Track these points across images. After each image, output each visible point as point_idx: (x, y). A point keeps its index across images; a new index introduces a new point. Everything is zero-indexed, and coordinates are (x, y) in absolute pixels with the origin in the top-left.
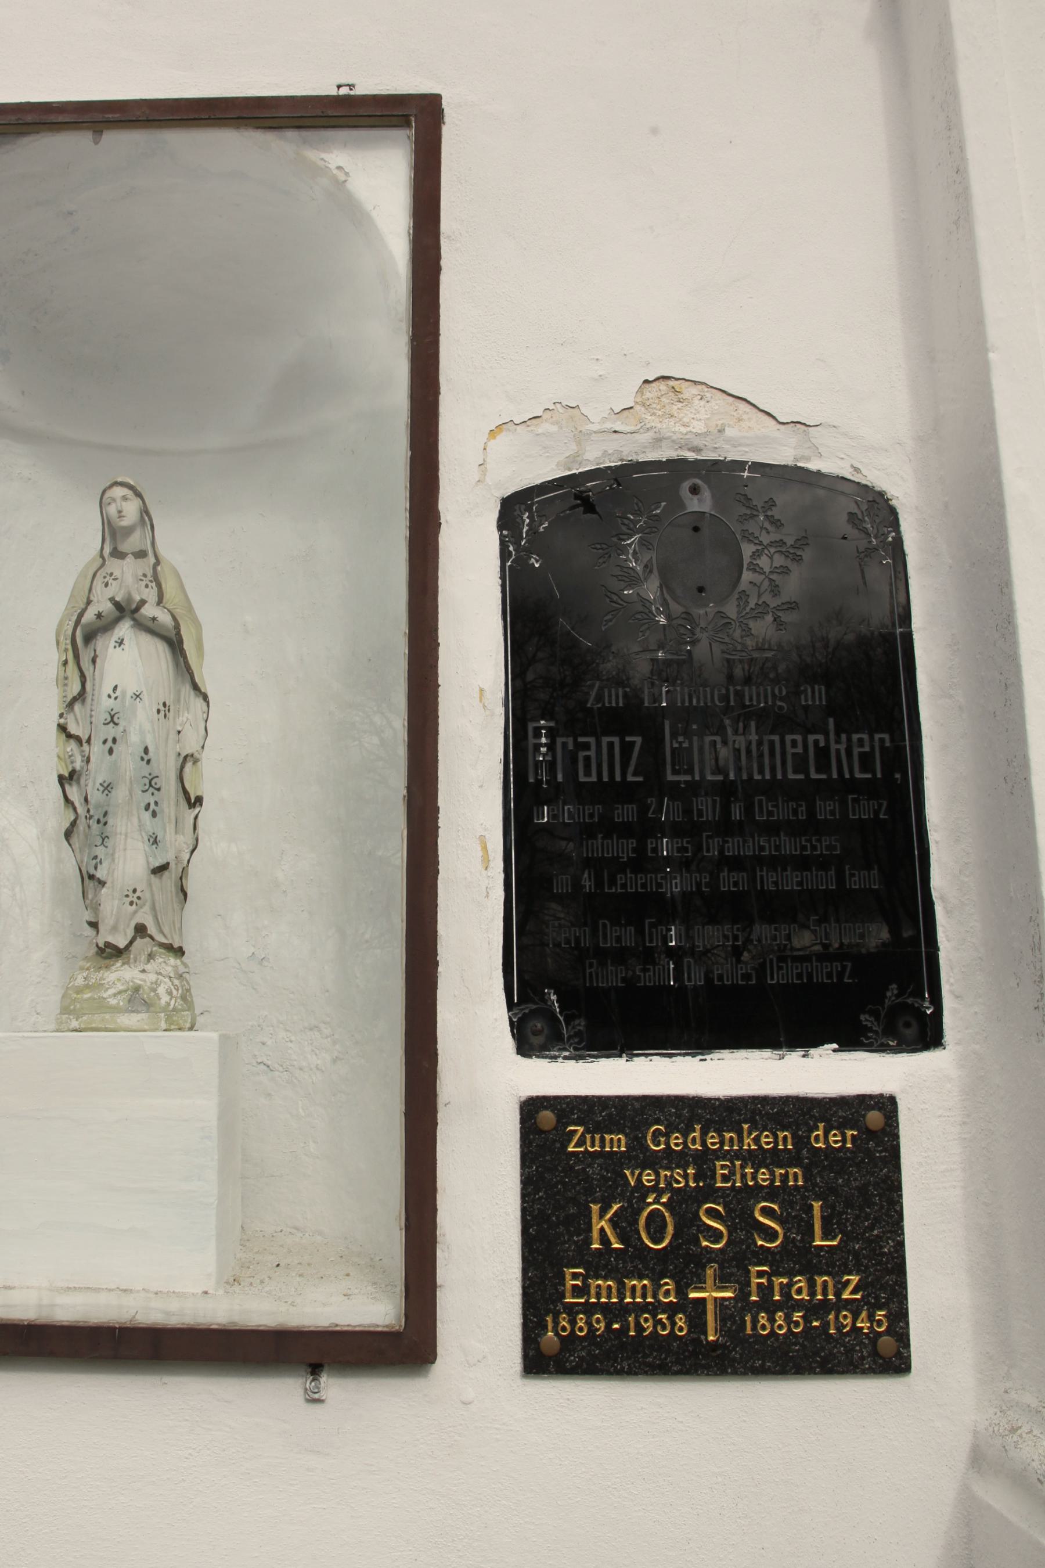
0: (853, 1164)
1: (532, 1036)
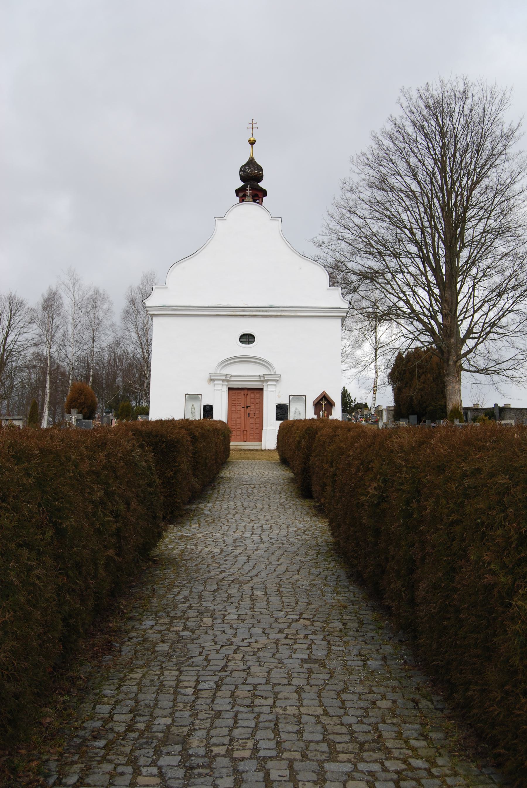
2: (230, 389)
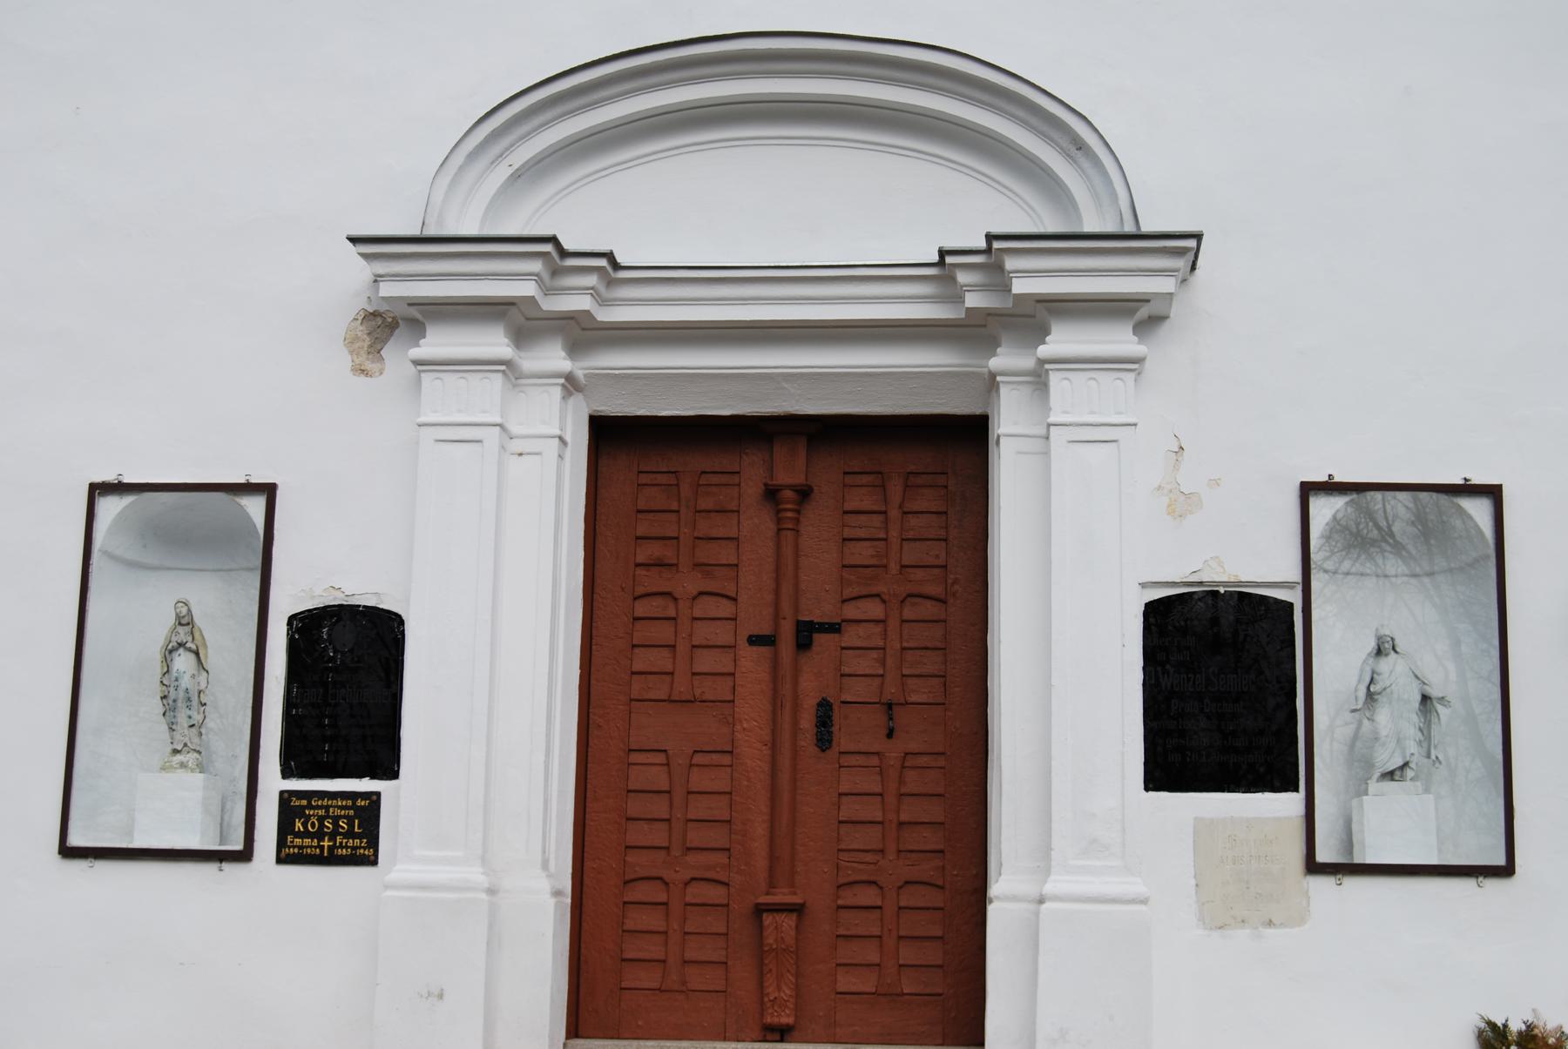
0: (368, 812)
1: (286, 773)
2: (608, 434)
